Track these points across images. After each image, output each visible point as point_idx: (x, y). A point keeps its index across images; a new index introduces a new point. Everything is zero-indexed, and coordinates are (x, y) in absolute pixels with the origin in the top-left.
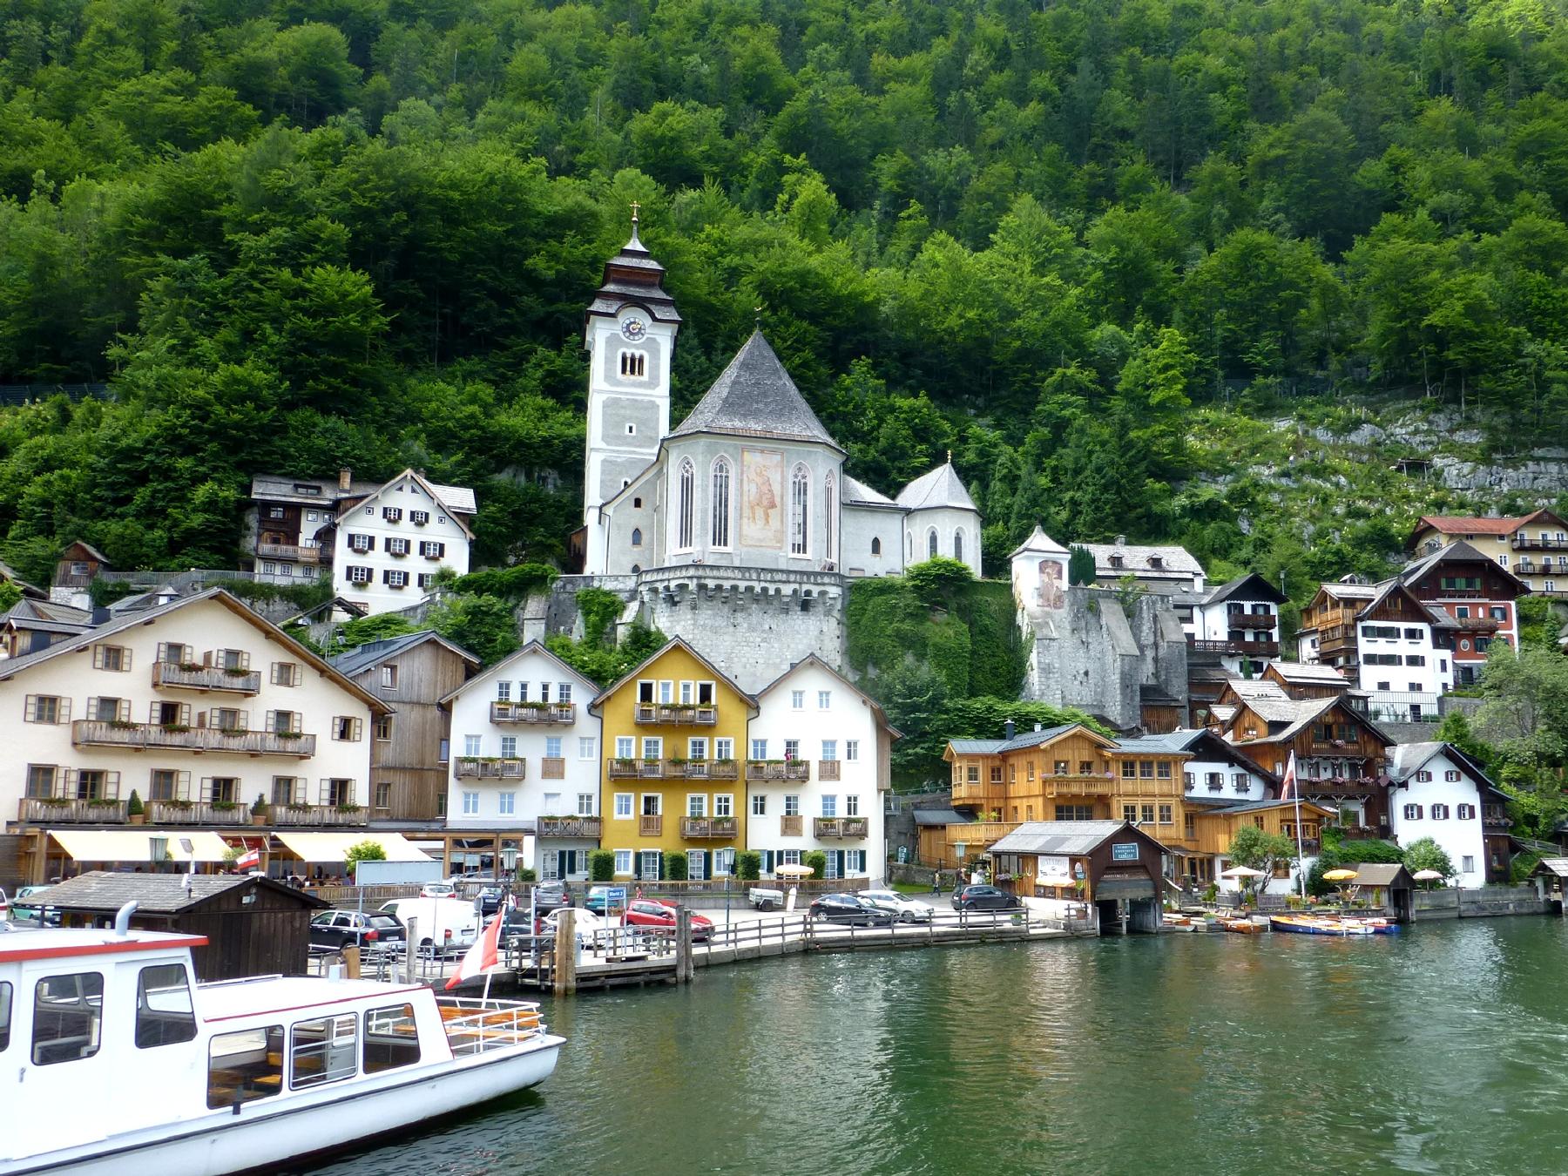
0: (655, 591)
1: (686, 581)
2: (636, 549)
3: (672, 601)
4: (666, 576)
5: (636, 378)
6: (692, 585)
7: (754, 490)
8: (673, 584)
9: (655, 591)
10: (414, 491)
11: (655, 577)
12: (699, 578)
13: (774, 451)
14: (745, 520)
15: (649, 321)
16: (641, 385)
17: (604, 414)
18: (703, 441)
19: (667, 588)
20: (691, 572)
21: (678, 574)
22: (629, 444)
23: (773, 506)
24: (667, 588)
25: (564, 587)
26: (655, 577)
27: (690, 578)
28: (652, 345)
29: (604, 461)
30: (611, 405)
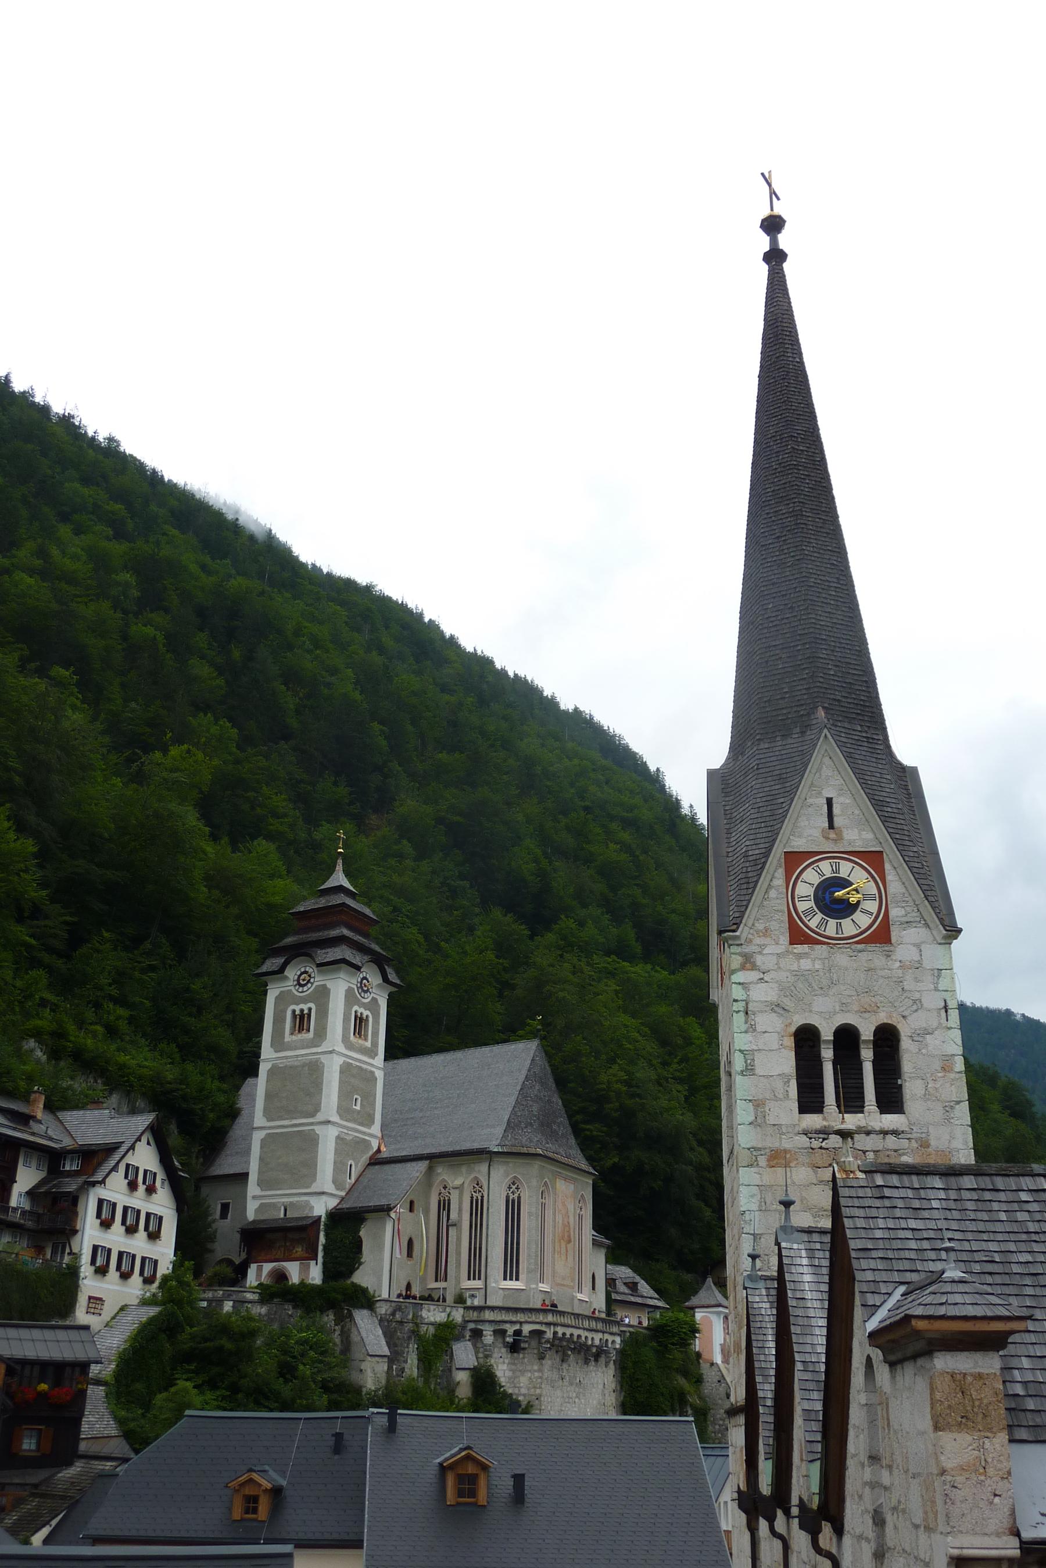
0: (500, 1333)
1: (543, 1328)
3: (514, 1348)
4: (520, 1317)
6: (549, 1335)
8: (527, 1329)
9: (502, 1333)
11: (504, 1316)
12: (555, 1325)
15: (380, 980)
16: (364, 1051)
18: (537, 1164)
19: (518, 1333)
20: (550, 1318)
21: (533, 1318)
22: (355, 1121)
24: (518, 1333)
26: (504, 1316)
27: (549, 1324)
28: (373, 1005)
30: (346, 1070)
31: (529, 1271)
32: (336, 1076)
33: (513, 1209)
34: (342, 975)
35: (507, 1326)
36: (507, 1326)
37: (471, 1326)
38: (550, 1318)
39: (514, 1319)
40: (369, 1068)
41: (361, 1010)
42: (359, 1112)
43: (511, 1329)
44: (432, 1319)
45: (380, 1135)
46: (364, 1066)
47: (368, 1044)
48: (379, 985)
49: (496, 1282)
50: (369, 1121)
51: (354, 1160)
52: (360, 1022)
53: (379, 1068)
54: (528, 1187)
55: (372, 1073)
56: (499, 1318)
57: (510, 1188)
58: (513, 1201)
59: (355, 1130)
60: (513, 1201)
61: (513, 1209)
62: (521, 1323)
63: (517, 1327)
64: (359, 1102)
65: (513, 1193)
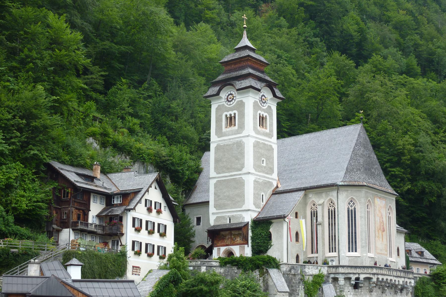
1: (371, 276)
2: (297, 244)
3: (356, 286)
4: (358, 271)
5: (264, 130)
6: (375, 279)
7: (378, 221)
8: (362, 277)
10: (156, 188)
12: (377, 274)
13: (385, 198)
14: (377, 239)
17: (254, 151)
18: (364, 190)
19: (357, 279)
20: (375, 271)
21: (366, 271)
22: (263, 172)
23: (384, 231)
24: (357, 279)
25: (290, 271)
26: (349, 270)
27: (374, 274)
29: (255, 181)
30: (257, 145)
31: (362, 247)
32: (252, 148)
33: (352, 216)
34: (251, 94)
35: (351, 276)
36: (351, 276)
37: (332, 276)
38: (375, 271)
39: (355, 272)
40: (269, 143)
41: (262, 113)
42: (265, 167)
43: (353, 277)
44: (311, 273)
45: (277, 179)
46: (266, 143)
47: (268, 131)
48: (271, 99)
49: (344, 253)
50: (272, 171)
51: (264, 192)
52: (262, 120)
53: (274, 143)
54: (360, 203)
55: (271, 146)
56: (347, 272)
57: (349, 204)
58: (352, 211)
59: (263, 177)
60: (352, 211)
61: (352, 216)
62: (359, 274)
63: (357, 276)
64: (265, 162)
65: (351, 206)
